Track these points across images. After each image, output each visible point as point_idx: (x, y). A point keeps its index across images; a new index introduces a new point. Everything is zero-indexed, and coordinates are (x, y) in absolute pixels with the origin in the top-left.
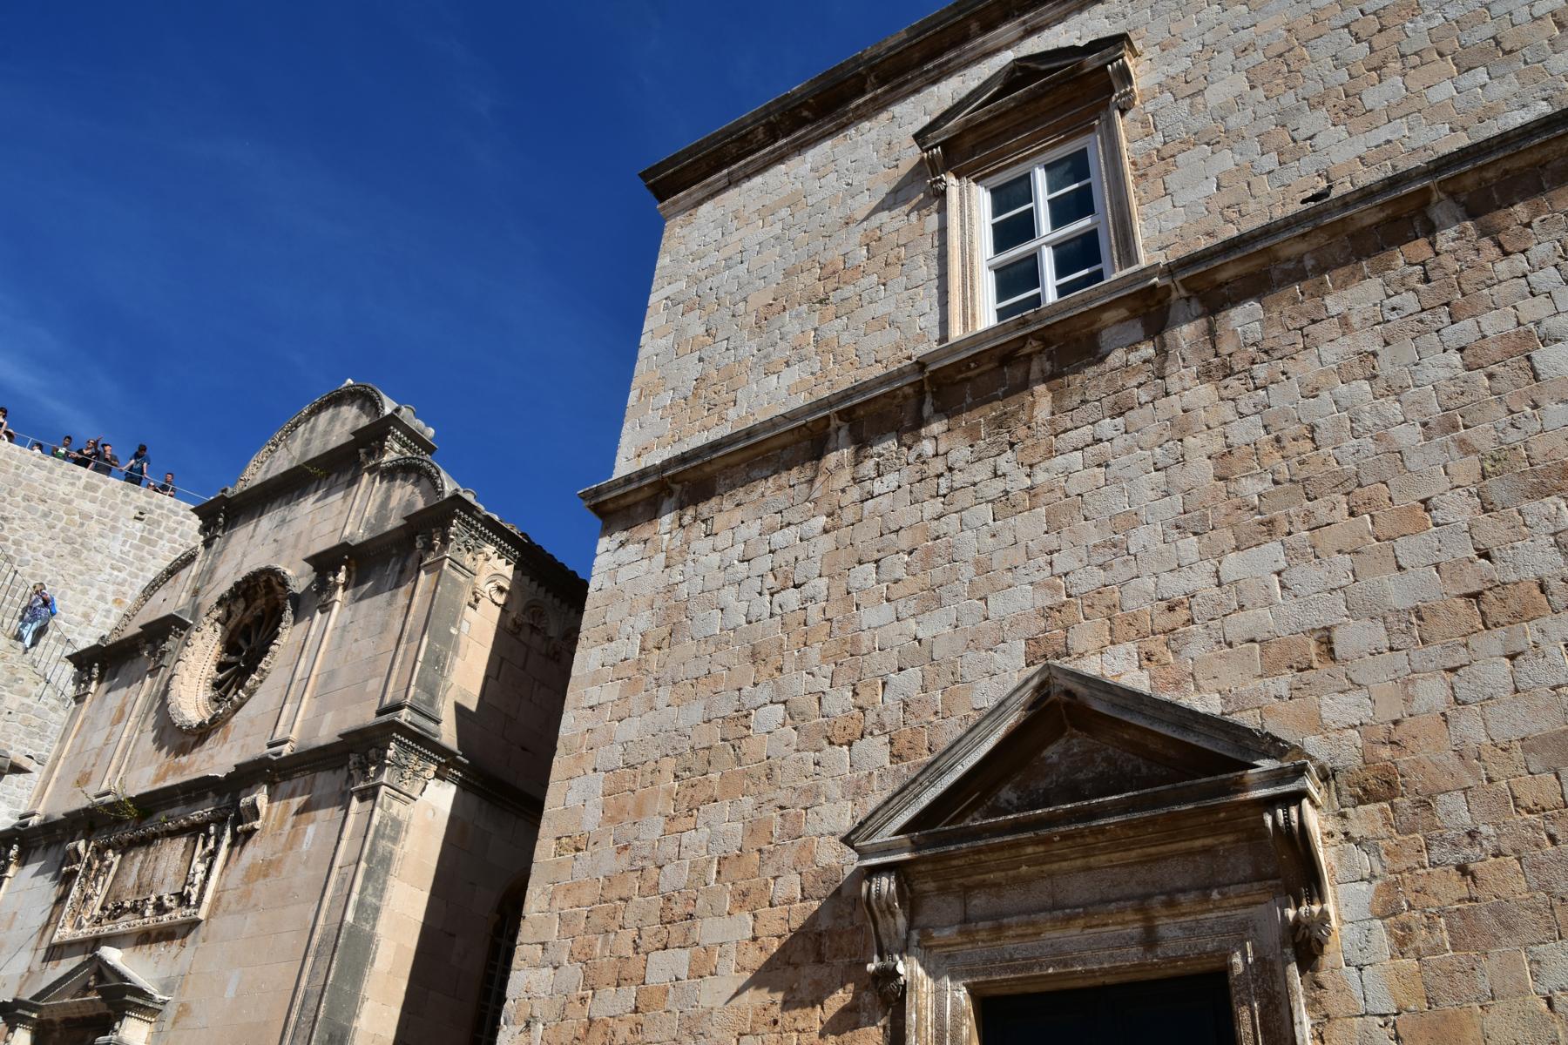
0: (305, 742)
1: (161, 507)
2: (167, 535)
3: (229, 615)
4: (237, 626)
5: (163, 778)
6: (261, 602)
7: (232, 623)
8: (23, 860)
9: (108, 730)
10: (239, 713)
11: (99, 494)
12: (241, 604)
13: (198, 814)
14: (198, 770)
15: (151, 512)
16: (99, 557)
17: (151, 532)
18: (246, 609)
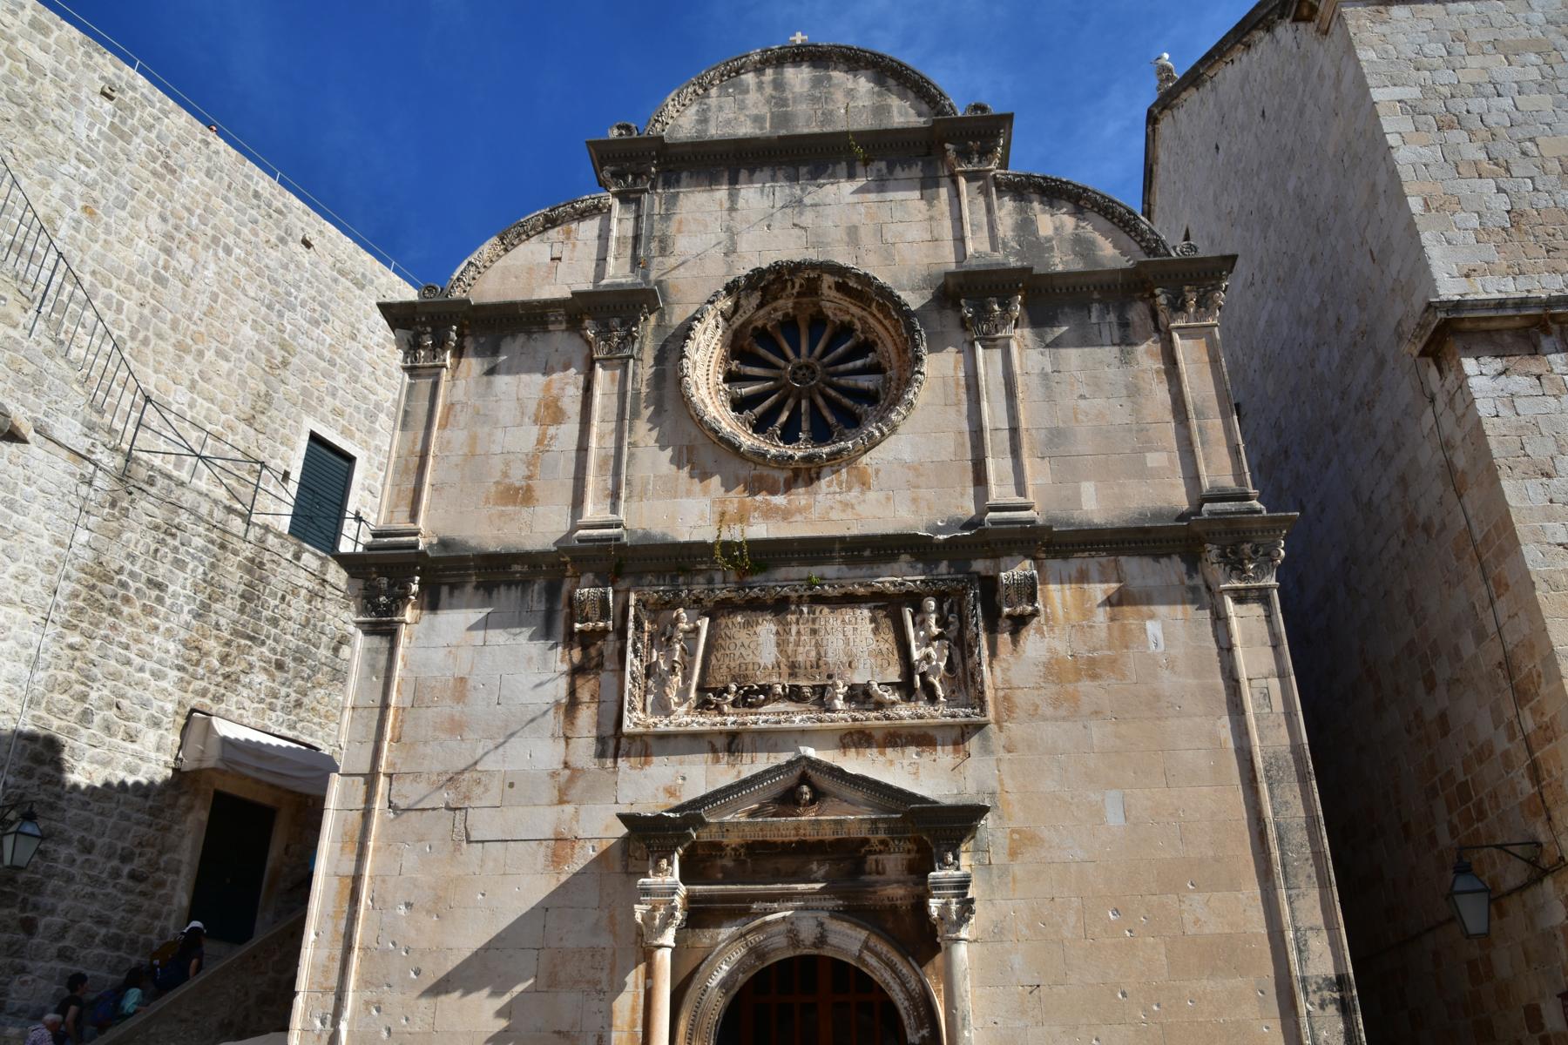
0: (1058, 513)
1: (134, 89)
2: (143, 132)
3: (737, 307)
4: (744, 325)
5: (742, 518)
6: (785, 304)
7: (738, 321)
8: (432, 603)
9: (535, 431)
11: (51, 41)
12: (755, 299)
13: (887, 579)
14: (825, 519)
15: (122, 91)
16: (60, 138)
17: (123, 121)
18: (760, 306)
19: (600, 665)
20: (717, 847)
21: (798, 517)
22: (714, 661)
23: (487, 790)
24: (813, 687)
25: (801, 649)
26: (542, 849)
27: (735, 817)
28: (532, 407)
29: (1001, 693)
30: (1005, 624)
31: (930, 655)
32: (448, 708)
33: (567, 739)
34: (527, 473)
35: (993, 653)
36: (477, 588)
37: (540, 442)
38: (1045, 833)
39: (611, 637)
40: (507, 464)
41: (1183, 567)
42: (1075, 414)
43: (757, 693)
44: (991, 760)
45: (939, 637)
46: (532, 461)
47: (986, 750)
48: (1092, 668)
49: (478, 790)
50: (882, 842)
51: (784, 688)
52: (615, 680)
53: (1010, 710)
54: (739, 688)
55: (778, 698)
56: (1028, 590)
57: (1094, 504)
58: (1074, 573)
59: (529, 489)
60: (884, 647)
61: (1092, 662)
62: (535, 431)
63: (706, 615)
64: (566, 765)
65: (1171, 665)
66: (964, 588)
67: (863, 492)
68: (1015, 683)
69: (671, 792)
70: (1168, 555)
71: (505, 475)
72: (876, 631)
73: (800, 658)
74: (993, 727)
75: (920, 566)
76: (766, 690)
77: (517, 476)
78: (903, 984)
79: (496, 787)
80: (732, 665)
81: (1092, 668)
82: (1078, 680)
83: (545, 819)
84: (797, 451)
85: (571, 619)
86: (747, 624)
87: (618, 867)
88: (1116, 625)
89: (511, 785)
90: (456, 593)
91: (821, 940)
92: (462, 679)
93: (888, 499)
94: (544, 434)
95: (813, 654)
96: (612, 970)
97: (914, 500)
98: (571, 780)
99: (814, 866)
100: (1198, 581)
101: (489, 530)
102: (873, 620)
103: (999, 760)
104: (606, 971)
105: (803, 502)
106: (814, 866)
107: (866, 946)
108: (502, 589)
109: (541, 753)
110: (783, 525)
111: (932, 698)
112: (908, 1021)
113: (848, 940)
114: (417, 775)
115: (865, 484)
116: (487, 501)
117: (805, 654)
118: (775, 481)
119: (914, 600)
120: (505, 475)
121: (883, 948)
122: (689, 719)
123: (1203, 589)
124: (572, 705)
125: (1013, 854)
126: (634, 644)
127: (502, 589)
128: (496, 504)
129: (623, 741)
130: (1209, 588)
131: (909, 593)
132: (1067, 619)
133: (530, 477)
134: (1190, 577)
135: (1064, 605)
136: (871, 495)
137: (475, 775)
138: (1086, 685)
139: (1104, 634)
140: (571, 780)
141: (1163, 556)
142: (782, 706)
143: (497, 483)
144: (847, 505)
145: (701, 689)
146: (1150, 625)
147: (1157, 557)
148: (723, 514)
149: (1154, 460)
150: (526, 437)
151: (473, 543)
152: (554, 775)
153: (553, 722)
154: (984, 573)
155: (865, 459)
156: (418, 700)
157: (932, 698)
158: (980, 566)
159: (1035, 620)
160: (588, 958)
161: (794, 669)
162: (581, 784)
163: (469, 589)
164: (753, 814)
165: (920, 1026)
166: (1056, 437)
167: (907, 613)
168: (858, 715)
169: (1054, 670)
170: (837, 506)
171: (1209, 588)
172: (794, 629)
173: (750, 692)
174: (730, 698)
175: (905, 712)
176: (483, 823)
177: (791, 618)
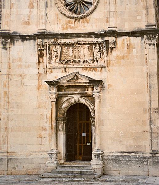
0: (121, 29)
5: (66, 28)
10: (90, 16)
19: (43, 56)
20: (63, 86)
21: (76, 29)
22: (62, 55)
23: (26, 77)
24: (78, 60)
25: (76, 53)
26: (36, 87)
27: (65, 82)
28: (28, 5)
29: (108, 62)
30: (110, 50)
31: (97, 55)
32: (18, 63)
33: (39, 68)
34: (28, 19)
35: (107, 55)
36: (21, 41)
37: (30, 12)
38: (114, 85)
39: (45, 51)
40: (24, 17)
41: (141, 39)
42: (126, 8)
43: (69, 61)
44: (106, 73)
45: (99, 51)
46: (29, 16)
47: (105, 71)
48: (123, 58)
49: (25, 77)
50: (88, 86)
51: (73, 60)
52: (46, 58)
53: (109, 64)
54: (66, 60)
55: (73, 62)
56: (115, 43)
57: (127, 28)
58: (122, 40)
59: (29, 22)
60: (90, 53)
61: (124, 56)
62: (29, 10)
63: (60, 47)
64: (39, 73)
65: (136, 57)
66: (103, 43)
67: (87, 24)
68: (111, 60)
69: (56, 78)
70: (139, 37)
71: (24, 19)
72: (89, 50)
73: (76, 55)
74: (107, 67)
75: (96, 38)
76: (70, 60)
77: (26, 19)
78: (91, 107)
79: (28, 76)
80: (65, 56)
81: (123, 58)
82: (121, 59)
83: (36, 82)
84: (76, 16)
85: (38, 47)
86: (67, 49)
87: (48, 89)
88: (128, 50)
89: (30, 76)
90: (18, 42)
91: (79, 101)
92: (20, 58)
93: (92, 25)
94: (31, 11)
95: (78, 54)
96: (48, 105)
97: (96, 26)
98: (40, 75)
99: (78, 89)
100: (143, 42)
101: (23, 31)
102: (88, 48)
103: (107, 73)
104: (47, 105)
105: (77, 26)
106: (78, 89)
107: (85, 102)
108: (26, 41)
109: (34, 71)
110: (74, 30)
111: (97, 62)
112: (92, 113)
113: (83, 101)
114: (15, 75)
115: (88, 22)
116: (21, 24)
117: (77, 55)
118: (72, 21)
119: (95, 44)
120: (24, 19)
121: (88, 102)
122: (58, 65)
123: (144, 43)
124: (39, 62)
125: (108, 88)
126: (48, 52)
127: (26, 41)
128: (23, 25)
129: (48, 69)
130: (145, 43)
131: (94, 43)
132: (120, 49)
133: (28, 20)
134: (142, 41)
135: (120, 46)
136: (88, 24)
137: (24, 74)
138: (122, 60)
139: (126, 51)
140: (40, 75)
141: (137, 37)
142: (73, 63)
143: (23, 20)
144: (84, 27)
145: (60, 60)
146: (134, 50)
147: (137, 37)
148: (63, 28)
149: (139, 18)
150: (27, 11)
151: (20, 32)
152: (37, 75)
153: (36, 65)
154: (106, 40)
155: (88, 17)
156: (13, 61)
157: (97, 62)
158: (106, 39)
159: (114, 49)
160: (44, 103)
161: (75, 56)
162: (41, 76)
163: (20, 41)
164: (68, 81)
165: (93, 113)
166: (122, 12)
167: (93, 47)
168: (85, 65)
169: (117, 58)
170: (83, 27)
171: (145, 43)
172: (75, 50)
173: (68, 61)
174: (65, 62)
175: (92, 65)
176: (26, 82)
177: (75, 48)
